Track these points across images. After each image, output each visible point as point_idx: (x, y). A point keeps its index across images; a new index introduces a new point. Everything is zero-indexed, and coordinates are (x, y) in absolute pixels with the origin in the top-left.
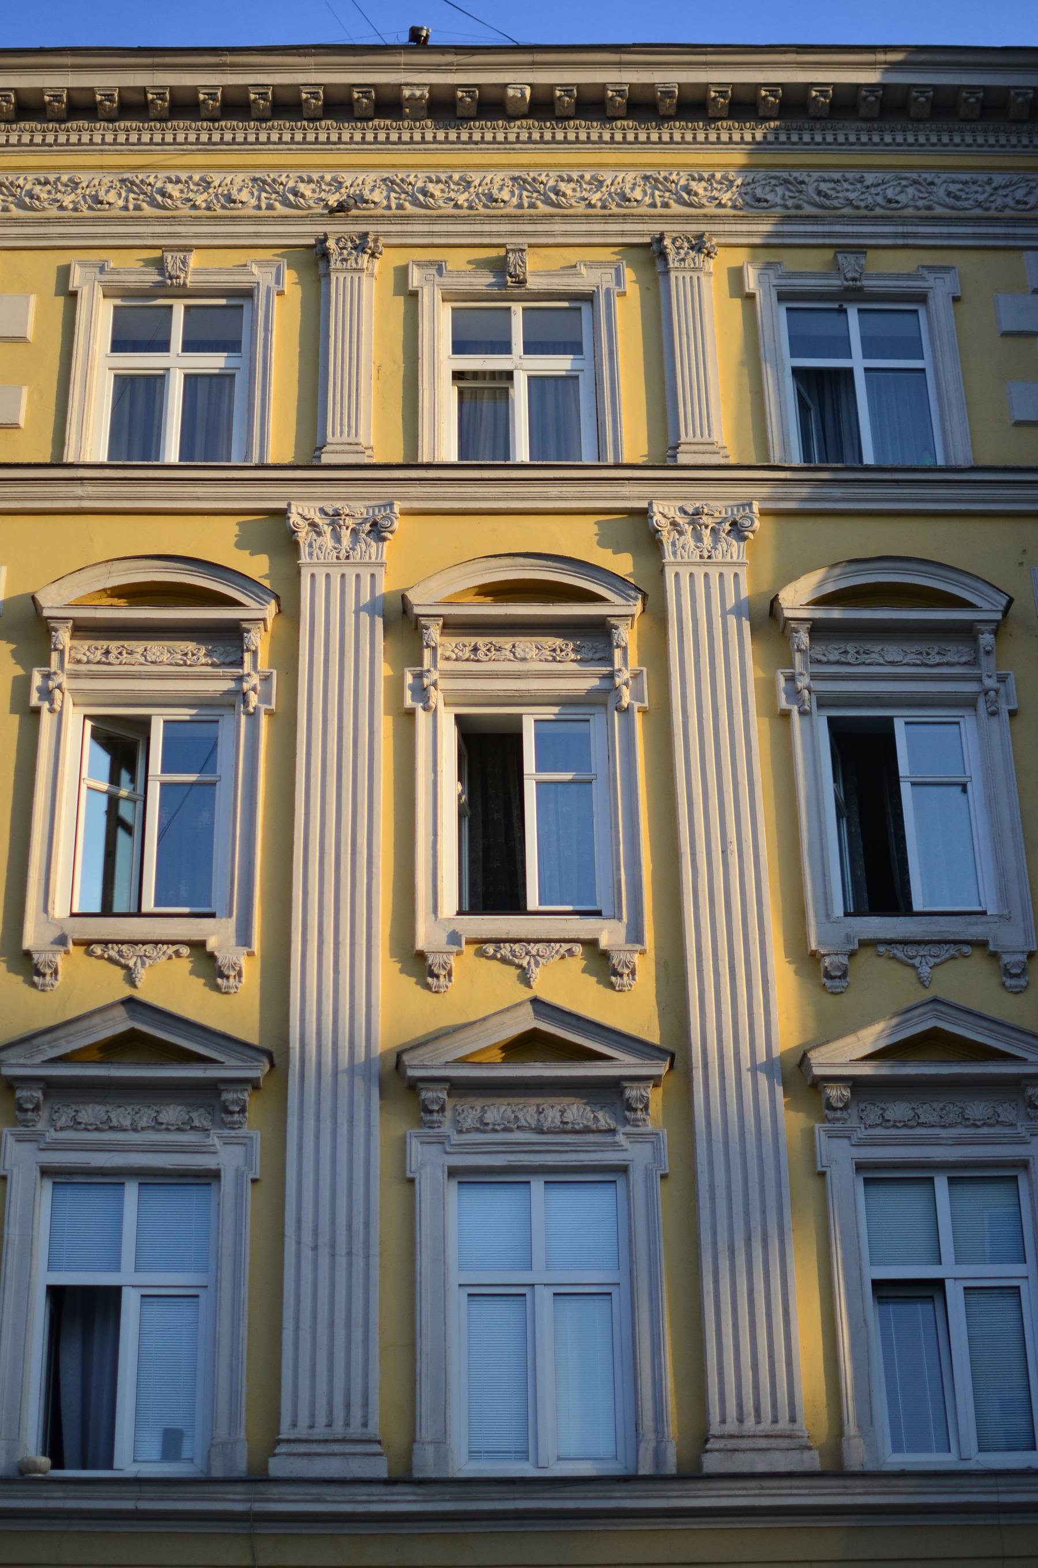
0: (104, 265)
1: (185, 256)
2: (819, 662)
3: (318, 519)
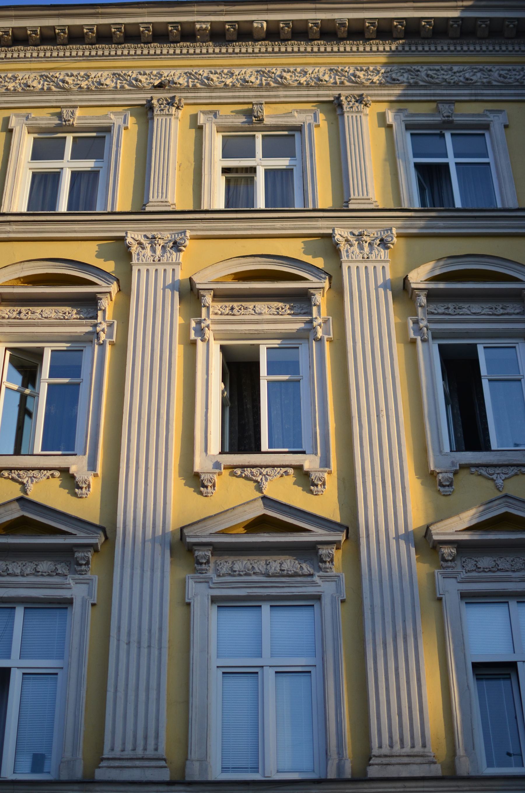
0: (28, 116)
1: (73, 111)
2: (433, 313)
3: (143, 240)
